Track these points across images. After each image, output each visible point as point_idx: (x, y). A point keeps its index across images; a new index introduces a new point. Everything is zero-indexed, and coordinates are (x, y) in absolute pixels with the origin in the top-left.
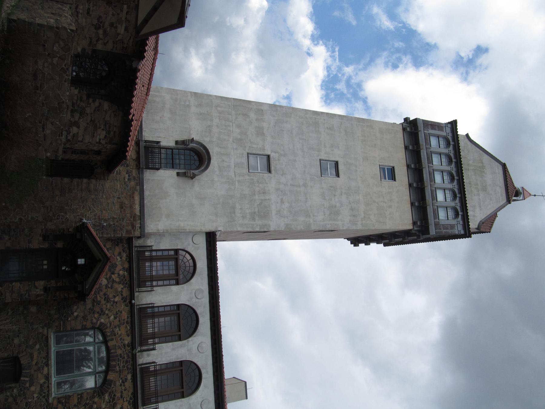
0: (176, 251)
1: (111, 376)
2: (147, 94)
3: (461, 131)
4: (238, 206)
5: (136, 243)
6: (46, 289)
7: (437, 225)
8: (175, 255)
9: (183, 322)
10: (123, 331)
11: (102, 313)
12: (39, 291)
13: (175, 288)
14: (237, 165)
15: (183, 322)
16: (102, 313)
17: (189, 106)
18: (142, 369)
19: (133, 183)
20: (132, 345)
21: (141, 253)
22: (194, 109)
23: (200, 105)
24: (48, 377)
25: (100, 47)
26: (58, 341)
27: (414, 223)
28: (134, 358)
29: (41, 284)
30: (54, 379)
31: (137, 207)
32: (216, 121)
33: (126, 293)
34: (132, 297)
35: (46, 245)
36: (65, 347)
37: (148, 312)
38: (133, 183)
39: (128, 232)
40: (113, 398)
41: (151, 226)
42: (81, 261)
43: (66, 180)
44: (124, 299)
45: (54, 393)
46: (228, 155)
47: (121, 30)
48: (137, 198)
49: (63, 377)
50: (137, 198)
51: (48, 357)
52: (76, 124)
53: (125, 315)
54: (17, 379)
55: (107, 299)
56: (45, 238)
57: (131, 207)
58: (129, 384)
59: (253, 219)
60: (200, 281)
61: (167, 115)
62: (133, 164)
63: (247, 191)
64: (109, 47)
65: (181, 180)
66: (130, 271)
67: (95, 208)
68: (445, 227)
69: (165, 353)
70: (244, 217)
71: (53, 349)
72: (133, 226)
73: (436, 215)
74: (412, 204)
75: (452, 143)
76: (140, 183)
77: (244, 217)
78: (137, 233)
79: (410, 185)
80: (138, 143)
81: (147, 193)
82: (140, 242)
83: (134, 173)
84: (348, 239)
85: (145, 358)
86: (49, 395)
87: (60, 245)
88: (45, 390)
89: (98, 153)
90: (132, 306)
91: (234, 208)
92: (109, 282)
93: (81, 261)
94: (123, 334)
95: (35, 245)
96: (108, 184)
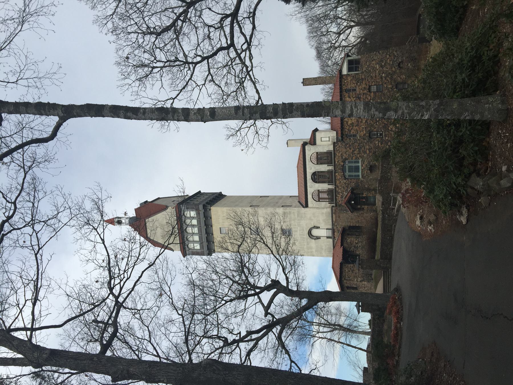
0: (319, 201)
1: (342, 164)
2: (333, 254)
3: (178, 253)
4: (296, 216)
5: (334, 205)
6: (363, 194)
7: (197, 210)
8: (319, 200)
9: (317, 177)
10: (338, 177)
11: (345, 183)
12: (365, 193)
13: (320, 189)
14: (297, 231)
15: (317, 177)
16: (345, 183)
17: (316, 251)
18: (332, 163)
19: (336, 224)
20: (335, 173)
21: (332, 200)
22: (314, 250)
23: (311, 252)
24: (362, 166)
25: (352, 265)
26: (359, 176)
27: (210, 210)
28: (335, 168)
29: (364, 195)
30: (360, 164)
31: (334, 217)
32: (305, 247)
33: (337, 189)
34: (335, 188)
35: (363, 207)
36: (357, 174)
37: (330, 182)
38: (336, 224)
39: (337, 209)
40: (342, 156)
41: (329, 210)
42: (353, 202)
43: (357, 225)
44: (338, 187)
45: (360, 161)
46: (300, 235)
47: (347, 270)
48: (334, 220)
49: (357, 165)
50: (334, 220)
51: (362, 172)
52: (356, 243)
53: (338, 182)
54: (371, 166)
55: (344, 187)
56: (363, 209)
57: (336, 217)
58: (337, 160)
59: (290, 212)
60: (310, 190)
61: (324, 248)
62: (336, 230)
63: (293, 222)
64: (349, 265)
65: (318, 226)
66: (336, 196)
67: (349, 218)
68: (192, 209)
69: (324, 168)
70: (294, 213)
71: (360, 174)
72: (335, 210)
73: (198, 214)
74: (211, 218)
75: (186, 247)
76: (333, 224)
77: (294, 213)
78: (334, 208)
79: (212, 226)
80: (334, 237)
81: (331, 221)
82: (333, 205)
83: (335, 228)
84: (225, 196)
85: (331, 168)
86: (362, 161)
87: (359, 207)
88: (363, 162)
89: (348, 235)
90: (335, 185)
91: (298, 216)
92: (343, 196)
93: (353, 202)
94: (338, 176)
95: (366, 207)
96: (344, 224)
